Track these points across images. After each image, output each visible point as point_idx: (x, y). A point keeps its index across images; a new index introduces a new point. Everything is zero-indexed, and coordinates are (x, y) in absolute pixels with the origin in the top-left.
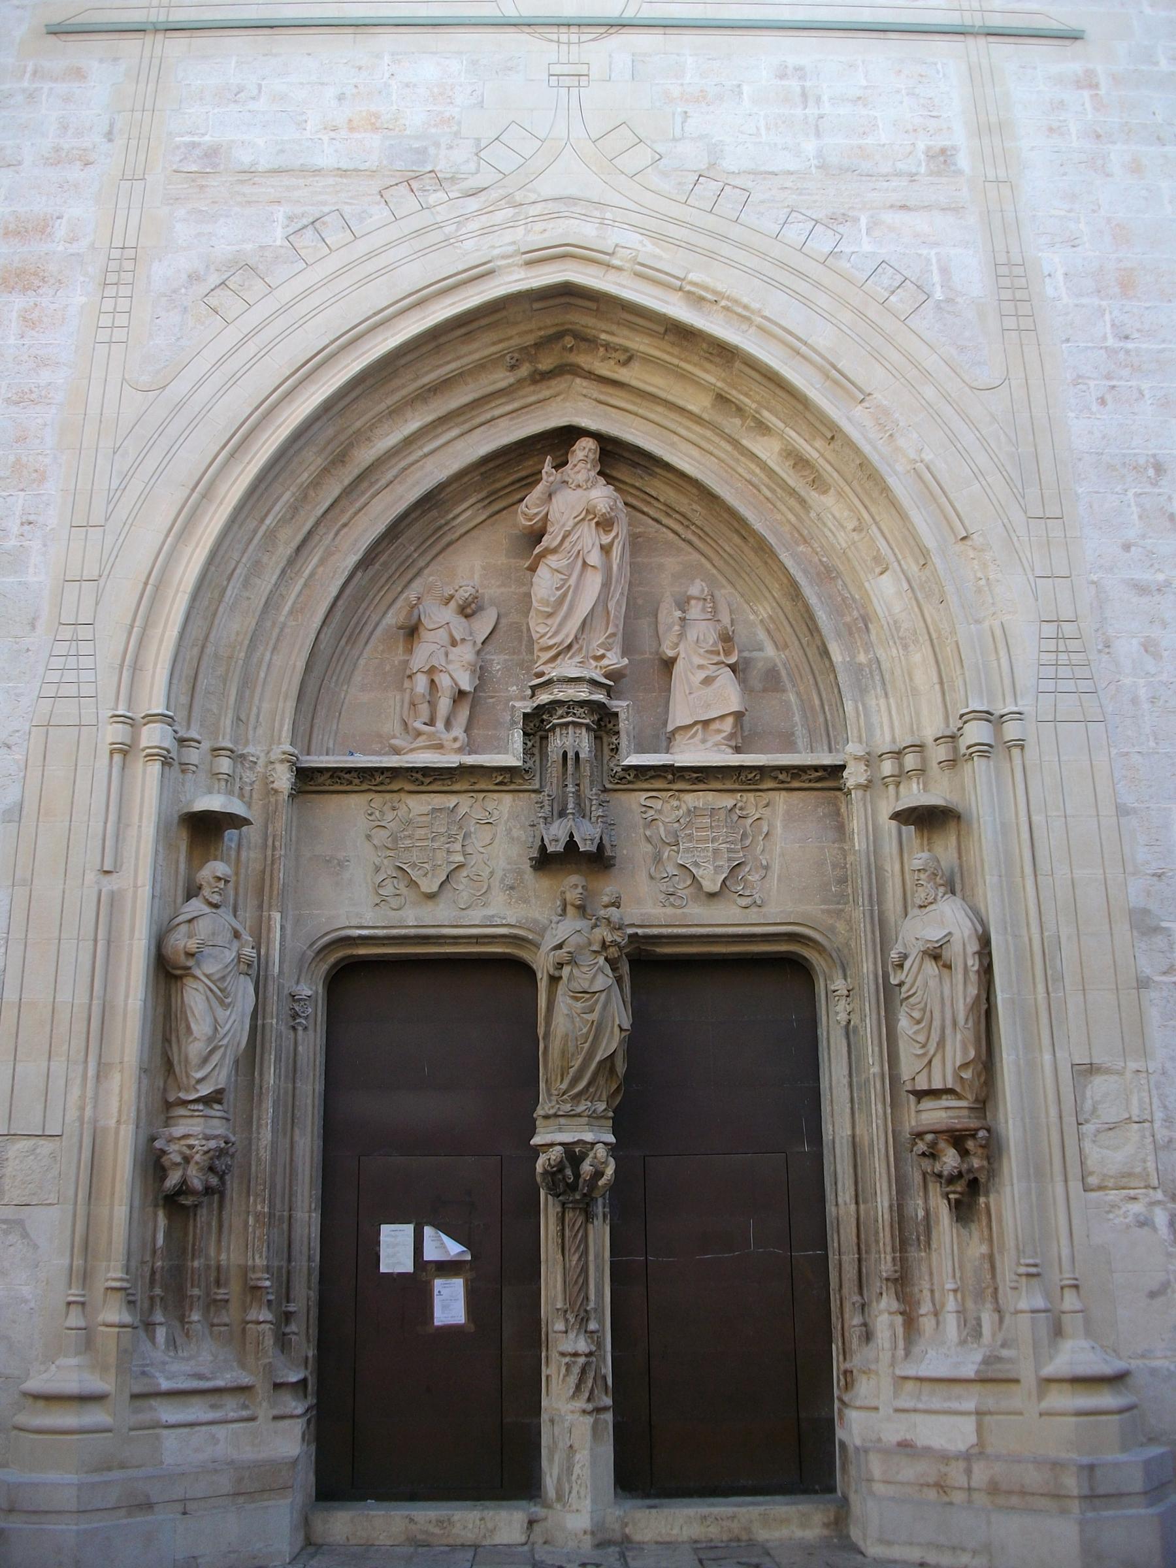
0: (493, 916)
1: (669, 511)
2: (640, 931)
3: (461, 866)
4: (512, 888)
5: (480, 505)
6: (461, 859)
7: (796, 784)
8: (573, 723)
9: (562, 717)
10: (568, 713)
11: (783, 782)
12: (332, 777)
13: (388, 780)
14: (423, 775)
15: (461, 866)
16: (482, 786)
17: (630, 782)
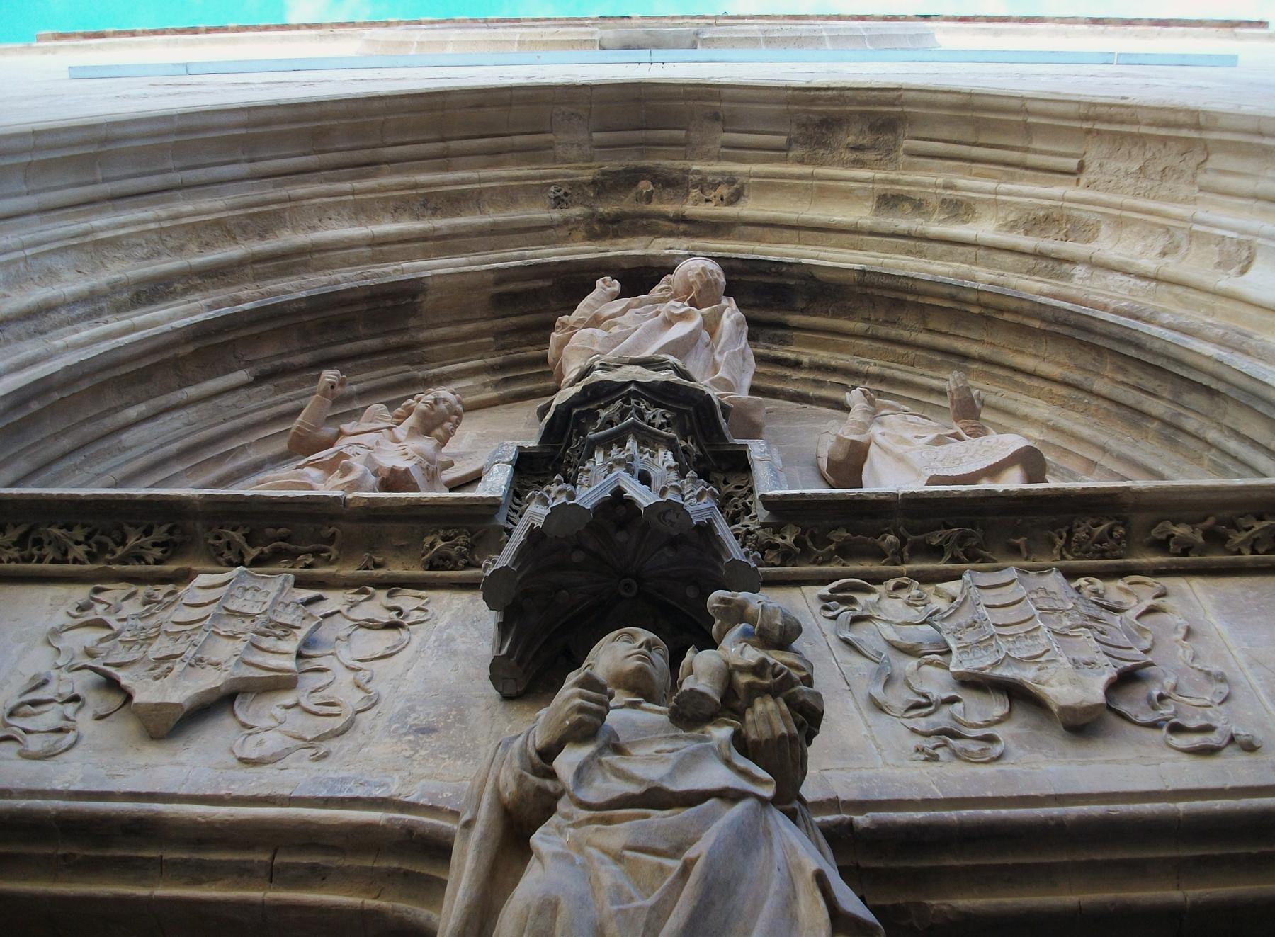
0: (344, 780)
1: (820, 377)
2: (862, 820)
3: (280, 684)
4: (427, 730)
5: (488, 378)
6: (289, 663)
7: (1216, 558)
8: (635, 429)
9: (610, 423)
10: (623, 414)
11: (1185, 553)
12: (21, 543)
13: (157, 552)
14: (251, 540)
15: (280, 684)
16: (396, 569)
17: (787, 557)
